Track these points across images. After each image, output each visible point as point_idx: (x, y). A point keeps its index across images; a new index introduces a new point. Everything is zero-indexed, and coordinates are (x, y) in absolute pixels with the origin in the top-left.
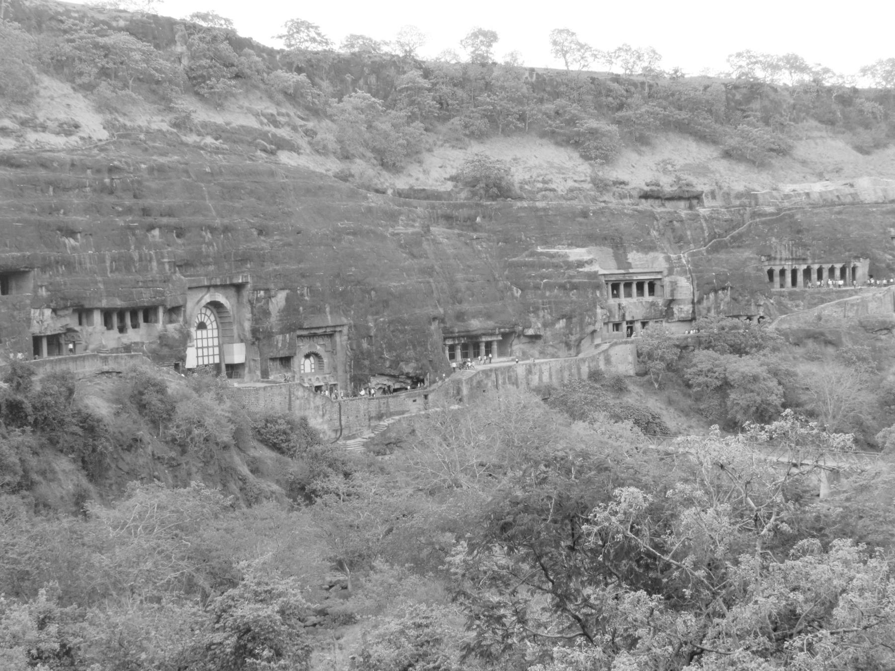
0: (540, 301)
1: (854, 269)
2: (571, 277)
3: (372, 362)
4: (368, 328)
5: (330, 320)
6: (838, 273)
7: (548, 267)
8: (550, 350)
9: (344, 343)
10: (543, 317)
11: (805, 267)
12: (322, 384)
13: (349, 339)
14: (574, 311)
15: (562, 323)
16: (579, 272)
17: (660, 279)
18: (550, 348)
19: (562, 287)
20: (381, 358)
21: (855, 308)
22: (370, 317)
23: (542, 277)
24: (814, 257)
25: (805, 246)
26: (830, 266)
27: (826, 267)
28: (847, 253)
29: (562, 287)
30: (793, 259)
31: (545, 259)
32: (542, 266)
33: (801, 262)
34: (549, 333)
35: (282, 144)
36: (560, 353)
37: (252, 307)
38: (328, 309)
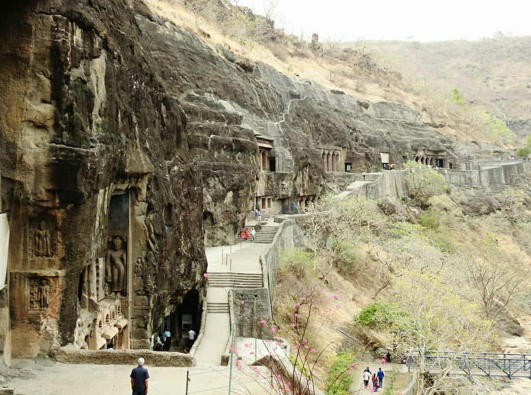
0: (212, 164)
2: (235, 134)
6: (330, 158)
8: (220, 234)
9: (141, 219)
10: (214, 187)
13: (150, 208)
14: (241, 181)
16: (241, 129)
17: (269, 149)
18: (220, 231)
19: (229, 147)
20: (178, 254)
23: (211, 132)
27: (327, 152)
28: (335, 142)
29: (229, 147)
31: (207, 108)
32: (206, 116)
34: (219, 210)
36: (229, 239)
37: (59, 79)
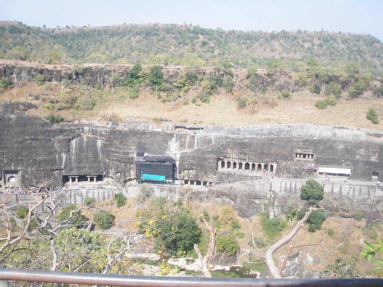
1: (272, 167)
3: (29, 182)
4: (28, 171)
5: (13, 168)
7: (117, 153)
11: (246, 163)
12: (13, 186)
15: (119, 174)
21: (249, 186)
22: (29, 168)
24: (249, 159)
25: (245, 154)
26: (258, 163)
29: (120, 161)
30: (239, 159)
33: (243, 160)
35: (30, 106)
38: (13, 165)
